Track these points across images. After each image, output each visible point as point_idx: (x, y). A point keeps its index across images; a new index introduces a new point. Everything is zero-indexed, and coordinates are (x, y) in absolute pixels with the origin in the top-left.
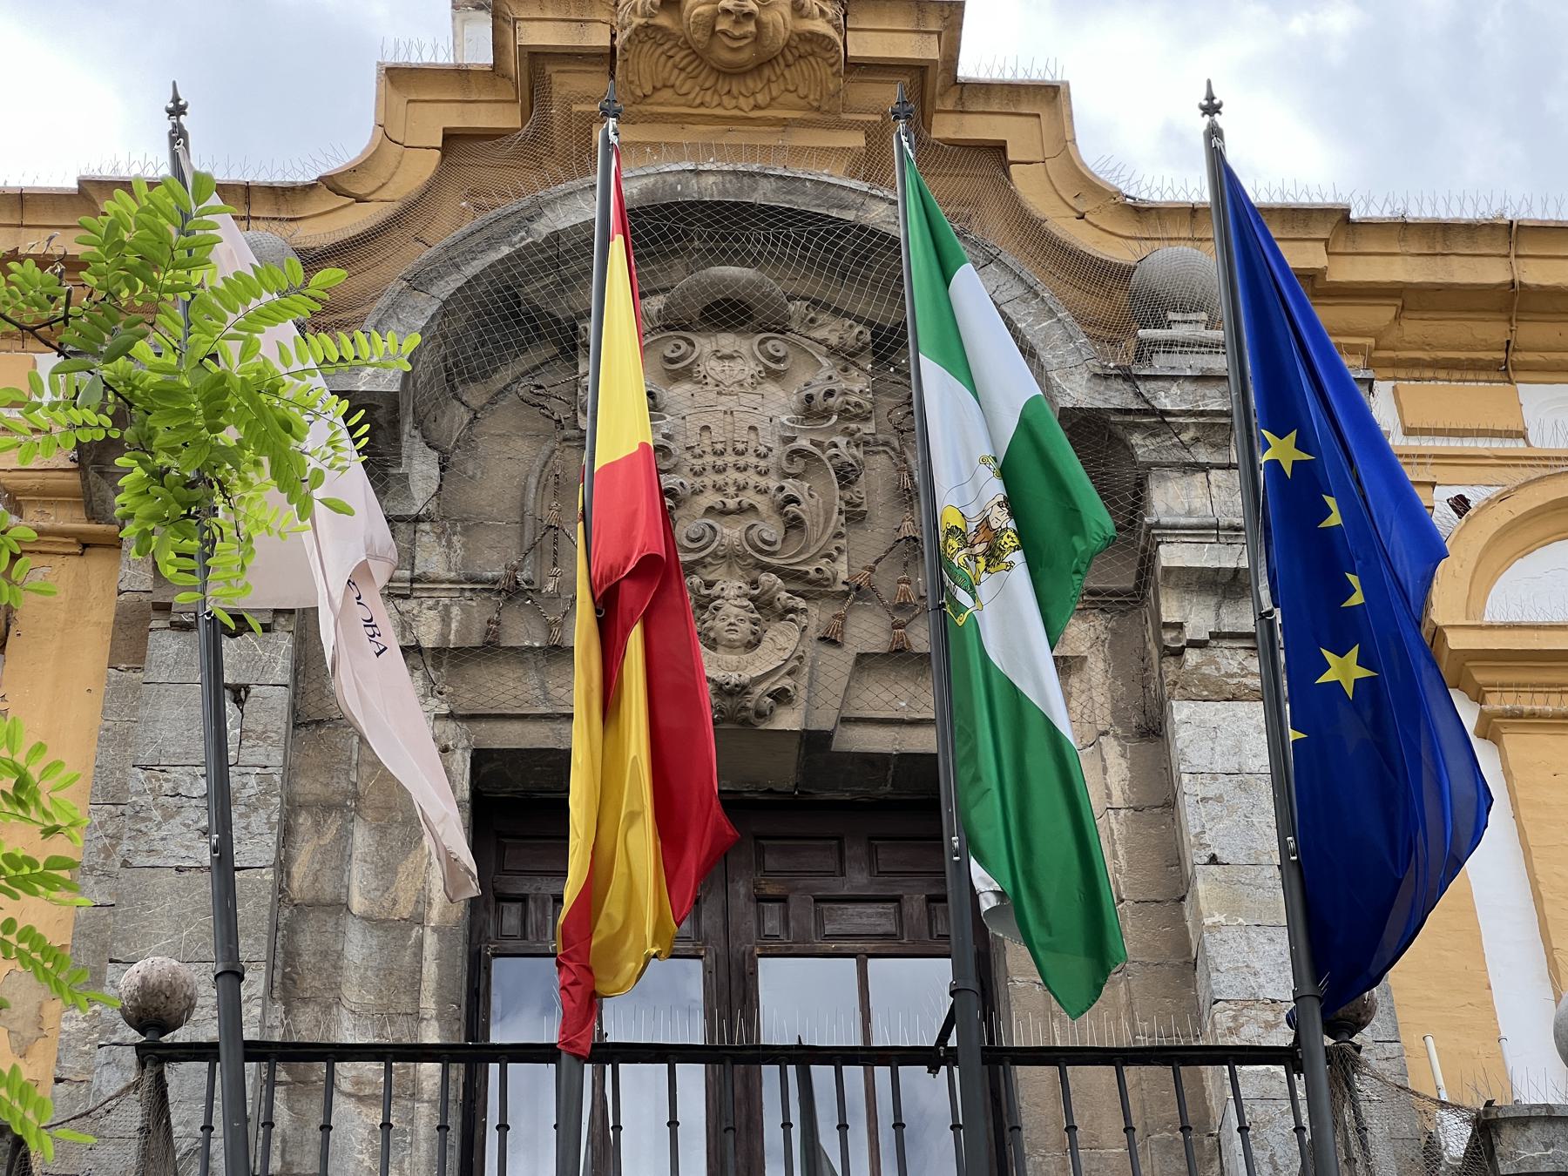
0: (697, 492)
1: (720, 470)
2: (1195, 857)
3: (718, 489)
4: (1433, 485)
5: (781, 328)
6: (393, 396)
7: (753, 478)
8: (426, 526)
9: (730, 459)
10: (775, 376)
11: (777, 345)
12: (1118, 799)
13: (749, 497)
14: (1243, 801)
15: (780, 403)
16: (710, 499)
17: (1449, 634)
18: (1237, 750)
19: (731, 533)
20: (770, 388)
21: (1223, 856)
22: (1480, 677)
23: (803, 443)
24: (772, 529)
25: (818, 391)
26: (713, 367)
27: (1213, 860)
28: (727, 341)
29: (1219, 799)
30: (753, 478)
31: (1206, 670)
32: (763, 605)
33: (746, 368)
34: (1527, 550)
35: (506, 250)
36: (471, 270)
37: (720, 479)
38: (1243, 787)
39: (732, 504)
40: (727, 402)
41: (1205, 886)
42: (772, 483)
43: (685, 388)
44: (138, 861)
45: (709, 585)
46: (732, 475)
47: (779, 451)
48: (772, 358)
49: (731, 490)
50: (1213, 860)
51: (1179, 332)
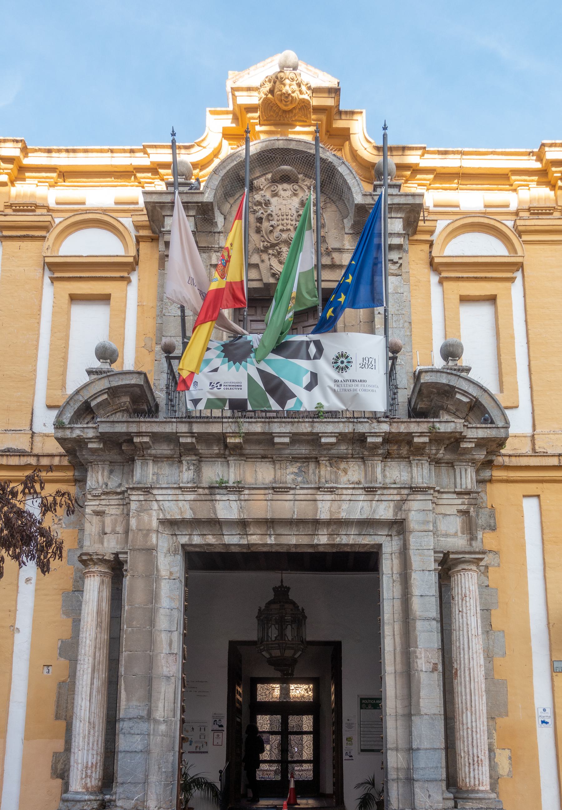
0: (278, 226)
1: (283, 220)
3: (283, 225)
4: (437, 220)
5: (296, 181)
6: (212, 203)
7: (289, 222)
8: (221, 234)
9: (285, 217)
10: (295, 195)
11: (296, 187)
13: (289, 227)
15: (296, 202)
16: (281, 227)
17: (435, 258)
19: (285, 236)
20: (294, 198)
22: (441, 269)
25: (304, 199)
26: (282, 193)
28: (285, 186)
30: (289, 222)
33: (289, 193)
34: (455, 237)
35: (235, 163)
36: (228, 168)
37: (283, 222)
39: (285, 228)
40: (284, 202)
42: (294, 223)
43: (276, 198)
44: (166, 314)
45: (280, 249)
46: (285, 221)
47: (296, 214)
48: (294, 190)
49: (285, 225)
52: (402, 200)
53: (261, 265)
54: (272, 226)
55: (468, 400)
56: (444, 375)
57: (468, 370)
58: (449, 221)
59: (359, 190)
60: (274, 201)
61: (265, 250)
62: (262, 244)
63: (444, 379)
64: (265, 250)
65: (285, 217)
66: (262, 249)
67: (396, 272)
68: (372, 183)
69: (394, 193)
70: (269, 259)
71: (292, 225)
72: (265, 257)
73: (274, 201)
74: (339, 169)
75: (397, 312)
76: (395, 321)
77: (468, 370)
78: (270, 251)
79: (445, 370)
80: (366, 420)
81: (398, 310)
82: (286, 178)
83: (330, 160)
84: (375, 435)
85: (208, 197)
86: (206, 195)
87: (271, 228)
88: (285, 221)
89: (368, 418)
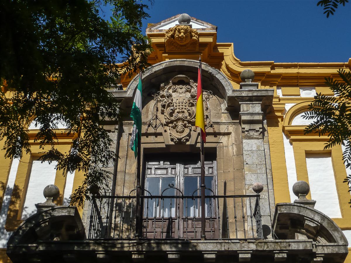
2: (245, 163)
3: (179, 109)
4: (285, 104)
5: (188, 84)
9: (181, 104)
12: (235, 154)
13: (183, 110)
14: (252, 155)
16: (178, 110)
18: (252, 147)
19: (180, 115)
21: (248, 163)
23: (191, 101)
24: (187, 114)
27: (247, 164)
28: (181, 86)
29: (249, 154)
31: (248, 135)
32: (185, 126)
38: (252, 152)
40: (180, 95)
41: (246, 167)
48: (187, 88)
49: (181, 109)
50: (247, 164)
51: (247, 83)
52: (259, 94)
53: (164, 133)
54: (172, 110)
55: (315, 225)
56: (296, 207)
57: (313, 203)
58: (294, 104)
59: (230, 88)
60: (174, 95)
61: (167, 124)
62: (165, 120)
63: (296, 211)
64: (167, 124)
65: (181, 104)
66: (165, 123)
67: (258, 137)
68: (239, 84)
69: (254, 90)
70: (170, 129)
71: (185, 109)
72: (167, 128)
73: (174, 95)
74: (217, 76)
75: (260, 163)
76: (259, 169)
77: (313, 203)
78: (171, 125)
79: (296, 204)
80: (238, 241)
81: (260, 162)
82: (181, 82)
83: (210, 71)
84: (246, 252)
85: (129, 94)
86: (128, 93)
87: (171, 111)
88: (181, 106)
89: (240, 240)
